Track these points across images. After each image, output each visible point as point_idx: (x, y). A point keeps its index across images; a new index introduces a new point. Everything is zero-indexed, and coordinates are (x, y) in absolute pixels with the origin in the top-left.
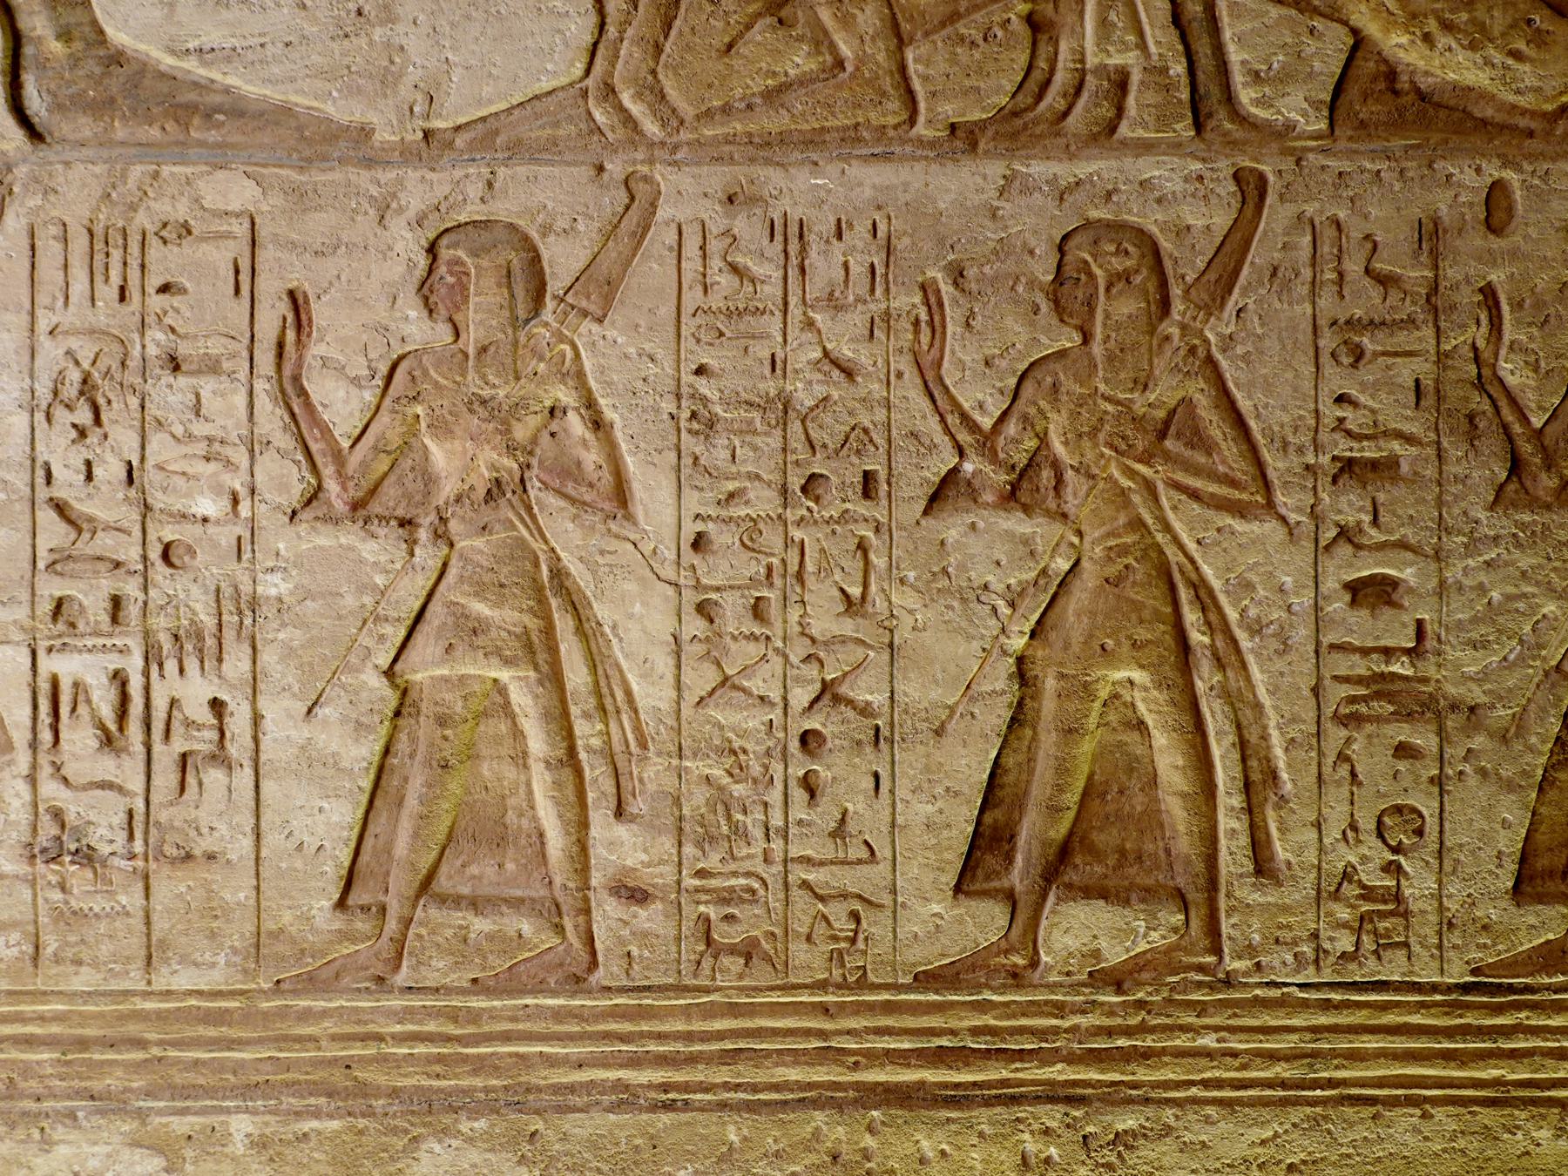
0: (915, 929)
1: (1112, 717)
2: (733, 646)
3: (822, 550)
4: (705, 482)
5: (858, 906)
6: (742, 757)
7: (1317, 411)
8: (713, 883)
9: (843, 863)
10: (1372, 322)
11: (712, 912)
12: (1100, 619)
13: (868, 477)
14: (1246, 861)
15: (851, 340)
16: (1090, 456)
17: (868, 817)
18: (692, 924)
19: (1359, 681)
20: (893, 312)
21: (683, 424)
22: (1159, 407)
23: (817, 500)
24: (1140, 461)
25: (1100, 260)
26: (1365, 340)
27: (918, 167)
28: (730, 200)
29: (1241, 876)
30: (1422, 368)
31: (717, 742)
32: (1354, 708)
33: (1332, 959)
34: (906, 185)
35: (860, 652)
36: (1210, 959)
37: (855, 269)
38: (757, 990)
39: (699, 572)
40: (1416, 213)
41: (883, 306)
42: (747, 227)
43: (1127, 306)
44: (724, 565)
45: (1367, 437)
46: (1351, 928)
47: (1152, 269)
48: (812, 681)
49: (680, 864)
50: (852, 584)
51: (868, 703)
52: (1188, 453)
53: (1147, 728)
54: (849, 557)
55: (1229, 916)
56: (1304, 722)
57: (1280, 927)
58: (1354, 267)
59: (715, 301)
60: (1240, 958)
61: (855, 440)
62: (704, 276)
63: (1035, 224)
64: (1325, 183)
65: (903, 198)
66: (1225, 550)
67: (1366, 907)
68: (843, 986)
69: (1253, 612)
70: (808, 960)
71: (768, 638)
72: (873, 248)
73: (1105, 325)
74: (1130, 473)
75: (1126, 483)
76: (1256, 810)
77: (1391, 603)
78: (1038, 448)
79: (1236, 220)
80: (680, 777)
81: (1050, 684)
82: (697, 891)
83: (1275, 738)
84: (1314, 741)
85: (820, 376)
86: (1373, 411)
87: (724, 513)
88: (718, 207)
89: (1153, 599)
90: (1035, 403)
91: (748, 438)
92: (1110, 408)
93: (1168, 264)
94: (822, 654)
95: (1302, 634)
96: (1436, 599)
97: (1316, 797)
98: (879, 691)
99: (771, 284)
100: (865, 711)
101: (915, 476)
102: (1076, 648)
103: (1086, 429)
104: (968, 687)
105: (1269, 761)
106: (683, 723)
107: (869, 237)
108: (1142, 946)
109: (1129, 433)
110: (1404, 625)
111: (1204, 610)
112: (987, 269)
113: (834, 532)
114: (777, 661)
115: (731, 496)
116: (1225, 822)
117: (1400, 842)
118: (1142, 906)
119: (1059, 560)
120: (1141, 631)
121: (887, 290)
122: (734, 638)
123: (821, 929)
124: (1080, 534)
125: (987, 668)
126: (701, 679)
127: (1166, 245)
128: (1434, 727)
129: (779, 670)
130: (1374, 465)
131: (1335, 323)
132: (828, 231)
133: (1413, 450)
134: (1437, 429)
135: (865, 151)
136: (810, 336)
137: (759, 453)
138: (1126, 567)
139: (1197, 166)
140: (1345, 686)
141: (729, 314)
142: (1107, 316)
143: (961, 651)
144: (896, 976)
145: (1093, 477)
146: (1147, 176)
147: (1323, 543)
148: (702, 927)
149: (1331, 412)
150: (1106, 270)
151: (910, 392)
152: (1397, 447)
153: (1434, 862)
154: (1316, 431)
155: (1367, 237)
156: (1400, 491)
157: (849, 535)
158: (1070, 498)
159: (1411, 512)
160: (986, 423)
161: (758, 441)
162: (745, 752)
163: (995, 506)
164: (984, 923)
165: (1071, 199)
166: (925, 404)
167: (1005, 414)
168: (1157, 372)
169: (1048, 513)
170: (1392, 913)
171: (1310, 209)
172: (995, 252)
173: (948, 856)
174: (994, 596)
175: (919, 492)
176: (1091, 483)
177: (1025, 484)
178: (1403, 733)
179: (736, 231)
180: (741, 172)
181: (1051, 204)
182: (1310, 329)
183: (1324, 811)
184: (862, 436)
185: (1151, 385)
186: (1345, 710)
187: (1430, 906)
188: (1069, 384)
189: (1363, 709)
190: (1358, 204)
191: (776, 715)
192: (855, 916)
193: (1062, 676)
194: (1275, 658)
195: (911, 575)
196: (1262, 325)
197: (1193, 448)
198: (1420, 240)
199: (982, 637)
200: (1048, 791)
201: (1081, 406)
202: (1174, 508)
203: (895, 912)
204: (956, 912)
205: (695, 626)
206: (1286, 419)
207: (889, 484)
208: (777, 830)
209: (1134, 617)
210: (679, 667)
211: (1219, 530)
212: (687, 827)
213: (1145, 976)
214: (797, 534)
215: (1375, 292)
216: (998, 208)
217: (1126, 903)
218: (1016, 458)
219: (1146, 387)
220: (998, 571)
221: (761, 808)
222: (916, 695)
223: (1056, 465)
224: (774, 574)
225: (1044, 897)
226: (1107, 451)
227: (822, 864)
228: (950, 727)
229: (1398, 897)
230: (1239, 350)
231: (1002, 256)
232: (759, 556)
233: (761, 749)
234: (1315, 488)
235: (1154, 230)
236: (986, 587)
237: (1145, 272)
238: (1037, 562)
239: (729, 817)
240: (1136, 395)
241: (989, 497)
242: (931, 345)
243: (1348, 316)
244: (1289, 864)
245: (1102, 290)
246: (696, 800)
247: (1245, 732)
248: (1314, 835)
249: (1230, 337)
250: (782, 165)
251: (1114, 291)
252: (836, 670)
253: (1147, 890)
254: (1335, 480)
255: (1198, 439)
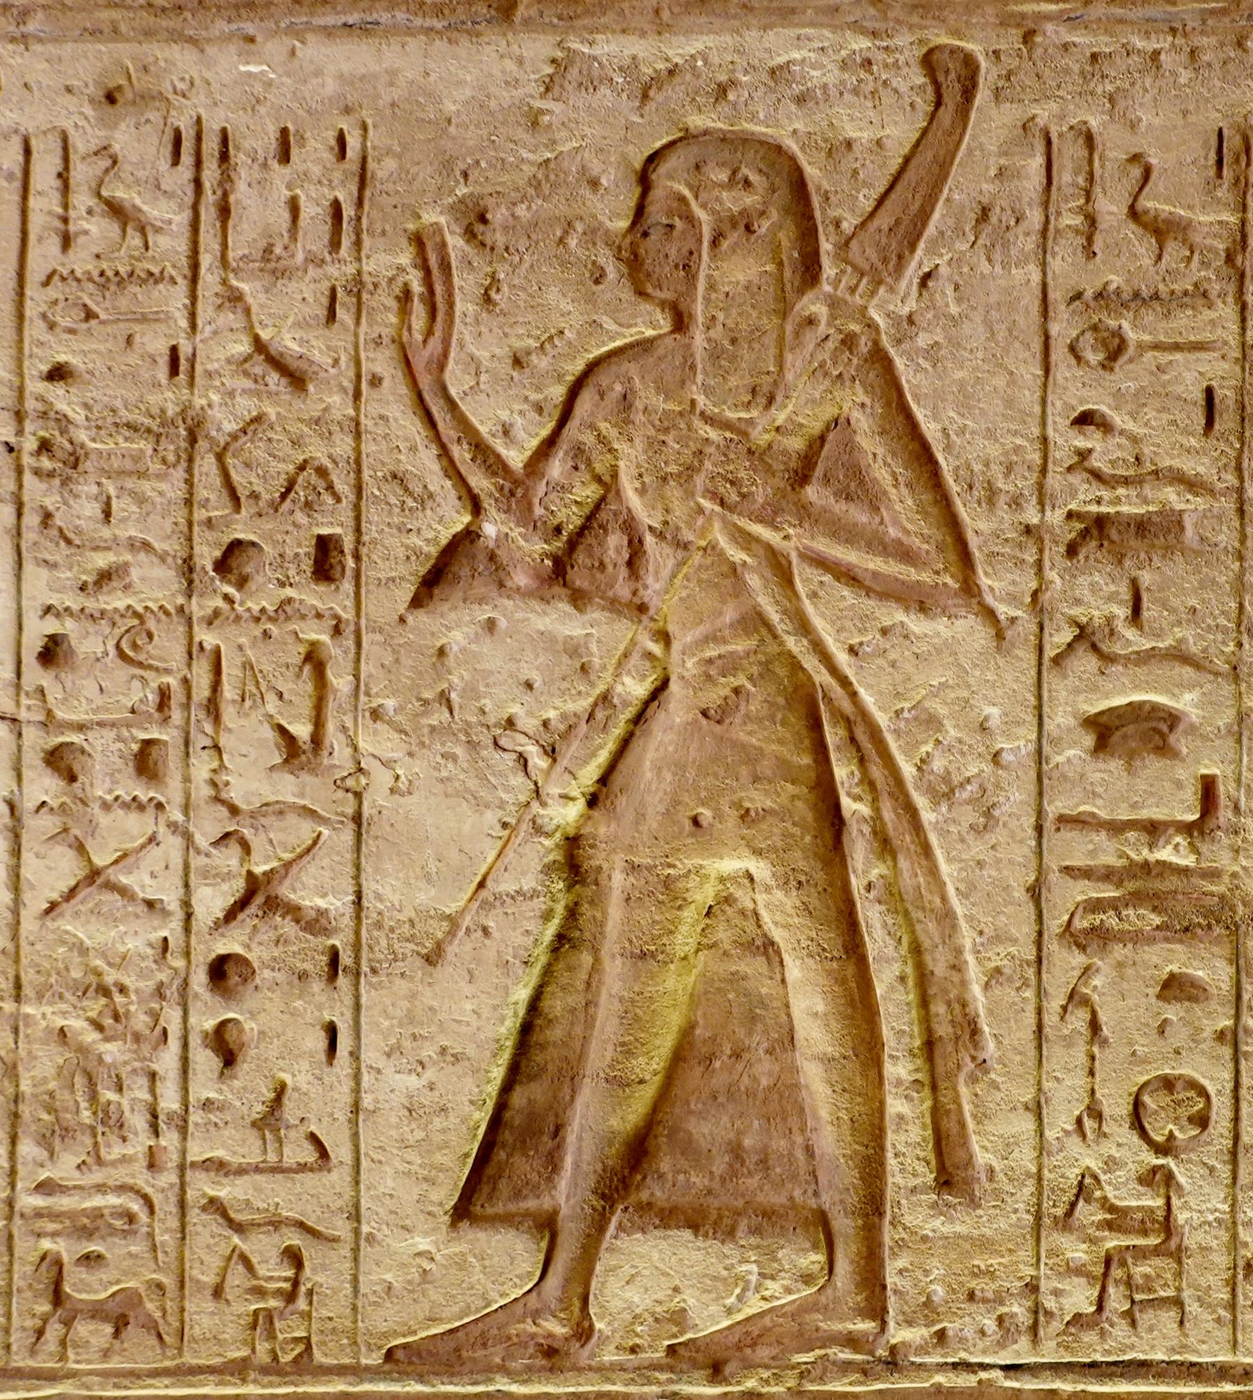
0: (389, 1277)
1: (722, 934)
2: (103, 819)
3: (248, 666)
4: (59, 553)
5: (294, 1239)
6: (119, 999)
7: (1044, 440)
8: (65, 1203)
9: (277, 1169)
10: (1136, 295)
11: (66, 1249)
12: (691, 774)
13: (324, 545)
14: (921, 1168)
15: (297, 325)
16: (680, 511)
17: (318, 1098)
18: (29, 1269)
19: (1108, 875)
20: (366, 278)
21: (27, 460)
22: (792, 433)
23: (242, 583)
24: (760, 520)
25: (703, 196)
26: (1126, 325)
27: (415, 44)
28: (111, 98)
29: (914, 1190)
30: (1218, 370)
31: (76, 974)
32: (1097, 919)
33: (1057, 1326)
34: (393, 73)
35: (304, 831)
36: (866, 1326)
37: (308, 211)
38: (135, 1375)
39: (50, 698)
40: (1214, 119)
41: (351, 270)
42: (139, 143)
43: (741, 270)
44: (90, 688)
45: (1126, 481)
46: (1088, 1275)
47: (786, 211)
48: (229, 876)
49: (13, 1172)
50: (296, 718)
51: (322, 913)
52: (840, 507)
53: (778, 953)
54: (290, 674)
55: (894, 1255)
56: (1015, 941)
57: (977, 1273)
58: (1110, 207)
59: (81, 261)
60: (910, 1323)
61: (300, 486)
62: (65, 220)
63: (600, 137)
64: (1067, 71)
65: (387, 95)
66: (893, 664)
67: (1113, 1242)
68: (273, 1369)
69: (938, 765)
70: (216, 1327)
71: (160, 806)
72: (337, 176)
73: (707, 300)
74: (746, 540)
75: (737, 555)
76: (942, 1085)
77: (1164, 749)
78: (603, 499)
79: (925, 132)
80: (16, 1031)
81: (618, 881)
82: (39, 1214)
83: (974, 973)
84: (1030, 973)
85: (248, 384)
86: (1134, 440)
87: (91, 605)
88: (89, 111)
89: (778, 742)
90: (592, 427)
91: (130, 483)
92: (713, 434)
93: (816, 201)
94: (247, 832)
95: (1015, 800)
96: (1230, 742)
97: (1032, 1063)
98: (335, 892)
99: (171, 234)
100: (316, 924)
101: (394, 542)
102: (653, 823)
103: (673, 468)
104: (481, 885)
105: (964, 1006)
106: (23, 943)
107: (329, 157)
108: (754, 1306)
109: (742, 474)
110: (1179, 785)
111: (862, 761)
112: (521, 210)
113: (266, 635)
114: (172, 846)
115: (104, 577)
116: (895, 1105)
117: (1171, 1136)
118: (754, 1240)
119: (627, 680)
120: (755, 795)
121: (358, 243)
122: (106, 806)
123: (237, 1278)
124: (665, 638)
125: (510, 854)
126: (51, 871)
127: (810, 171)
128: (1226, 950)
129: (177, 860)
130: (1141, 526)
131: (1078, 296)
132: (266, 150)
133: (1200, 503)
134: (1239, 468)
135: (331, 20)
136: (231, 318)
137: (147, 507)
138: (737, 691)
139: (861, 44)
140: (1084, 883)
141: (104, 287)
142: (712, 287)
143: (467, 827)
144: (356, 1355)
145: (686, 546)
146: (781, 60)
147: (1050, 652)
148: (46, 1274)
149: (1067, 441)
150: (713, 212)
151: (391, 410)
152: (1173, 497)
153: (1224, 1171)
154: (1044, 471)
155: (1135, 158)
156: (1177, 568)
157: (290, 639)
158: (650, 580)
159: (1193, 602)
160: (516, 458)
161: (146, 487)
162: (123, 990)
163: (526, 594)
164: (501, 1265)
165: (660, 98)
166: (410, 426)
167: (550, 443)
168: (789, 376)
169: (614, 606)
170: (1157, 1251)
171: (1043, 113)
172: (535, 183)
173: (439, 1158)
174: (521, 739)
175: (403, 570)
176: (680, 554)
177: (581, 557)
178: (1175, 959)
179: (116, 147)
180: (125, 52)
181: (627, 106)
182: (1035, 308)
183: (1046, 1085)
184: (314, 479)
185: (779, 398)
186: (1081, 923)
187: (1217, 1240)
188: (649, 397)
189: (1111, 920)
190: (1121, 104)
191: (172, 929)
192: (294, 1257)
193: (633, 868)
194: (970, 838)
195: (390, 703)
196: (959, 300)
197: (849, 498)
198: (1220, 163)
199: (502, 805)
200: (609, 1055)
201: (666, 431)
202: (814, 595)
203: (356, 1250)
204: (455, 1248)
205: (42, 786)
206: (994, 451)
207: (357, 557)
208: (170, 1116)
209: (744, 771)
210: (16, 852)
211: (884, 632)
212: (25, 1110)
213: (763, 1353)
214: (209, 638)
215: (1144, 248)
216: (541, 112)
217: (731, 1233)
218: (561, 516)
219: (771, 400)
220: (528, 697)
221: (143, 1081)
222: (396, 899)
223: (629, 526)
224: (173, 703)
225: (601, 1228)
226: (707, 504)
227: (241, 1171)
228: (451, 950)
229: (1167, 1225)
230: (923, 340)
231: (546, 188)
232: (148, 674)
233: (148, 985)
234: (1039, 564)
235: (792, 146)
236: (510, 723)
237: (774, 215)
238: (592, 685)
239: (93, 1097)
240: (754, 413)
241: (521, 579)
242: (429, 333)
243: (1098, 285)
244: (991, 1171)
245: (706, 244)
246: (41, 1068)
247: (927, 958)
248: (1027, 1124)
249: (910, 320)
250: (192, 41)
251: (725, 245)
252: (267, 859)
253: (768, 1214)
254: (1072, 550)
255: (857, 486)
